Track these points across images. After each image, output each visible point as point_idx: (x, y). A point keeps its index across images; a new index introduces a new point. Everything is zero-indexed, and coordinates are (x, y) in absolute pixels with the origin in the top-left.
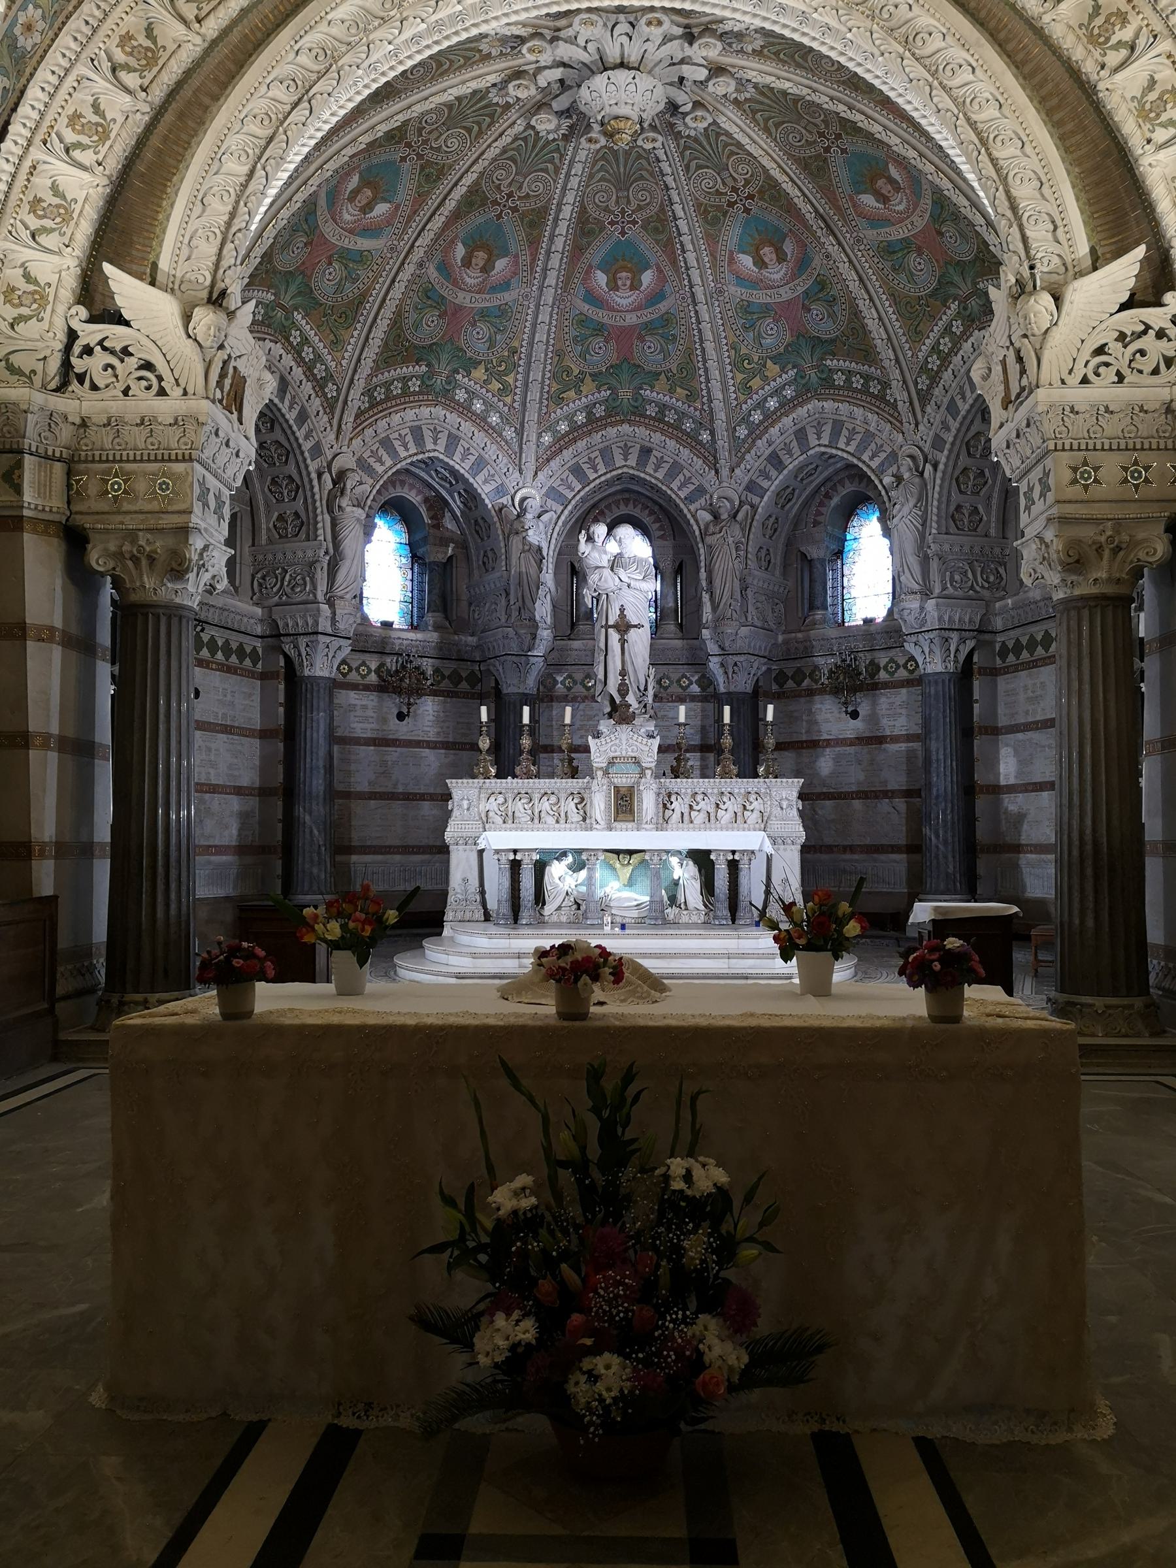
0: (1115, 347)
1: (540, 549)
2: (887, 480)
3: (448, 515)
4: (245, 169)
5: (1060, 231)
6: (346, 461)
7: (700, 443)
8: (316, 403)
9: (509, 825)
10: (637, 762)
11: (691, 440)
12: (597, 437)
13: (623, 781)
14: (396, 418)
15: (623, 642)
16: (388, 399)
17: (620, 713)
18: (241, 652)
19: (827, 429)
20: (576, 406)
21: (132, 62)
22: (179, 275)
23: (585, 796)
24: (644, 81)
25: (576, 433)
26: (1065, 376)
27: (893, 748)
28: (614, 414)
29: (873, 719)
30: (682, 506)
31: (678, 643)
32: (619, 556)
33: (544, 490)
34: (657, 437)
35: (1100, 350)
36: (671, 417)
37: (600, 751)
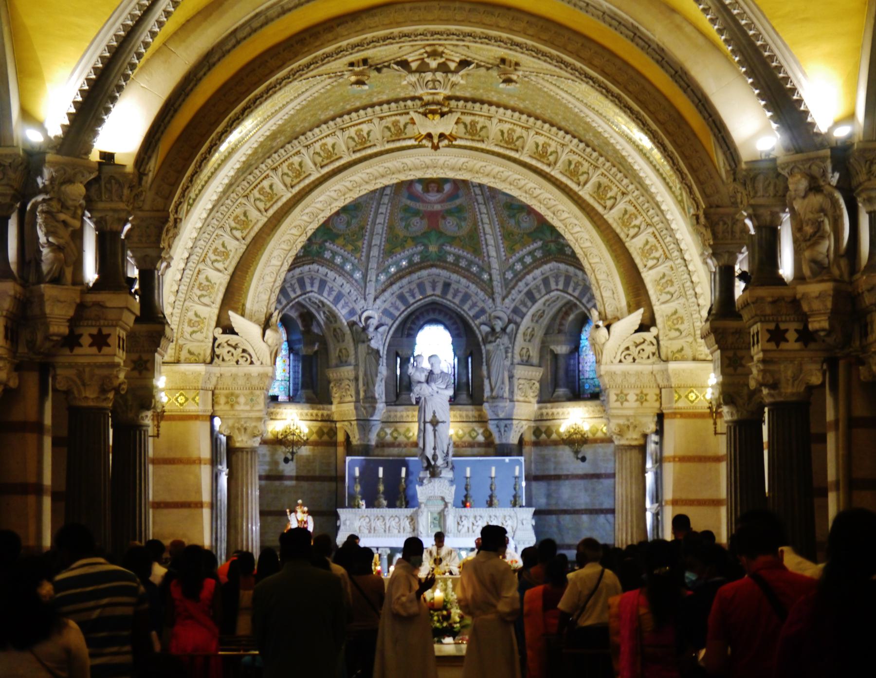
0: (632, 348)
1: (378, 352)
3: (315, 323)
4: (280, 263)
5: (615, 295)
7: (483, 280)
9: (372, 534)
10: (443, 499)
11: (476, 279)
12: (415, 276)
15: (435, 431)
17: (434, 473)
21: (238, 226)
22: (254, 309)
23: (415, 518)
25: (401, 274)
26: (613, 359)
28: (426, 262)
30: (471, 321)
32: (431, 372)
33: (380, 311)
34: (454, 277)
35: (628, 348)
36: (463, 264)
37: (422, 492)
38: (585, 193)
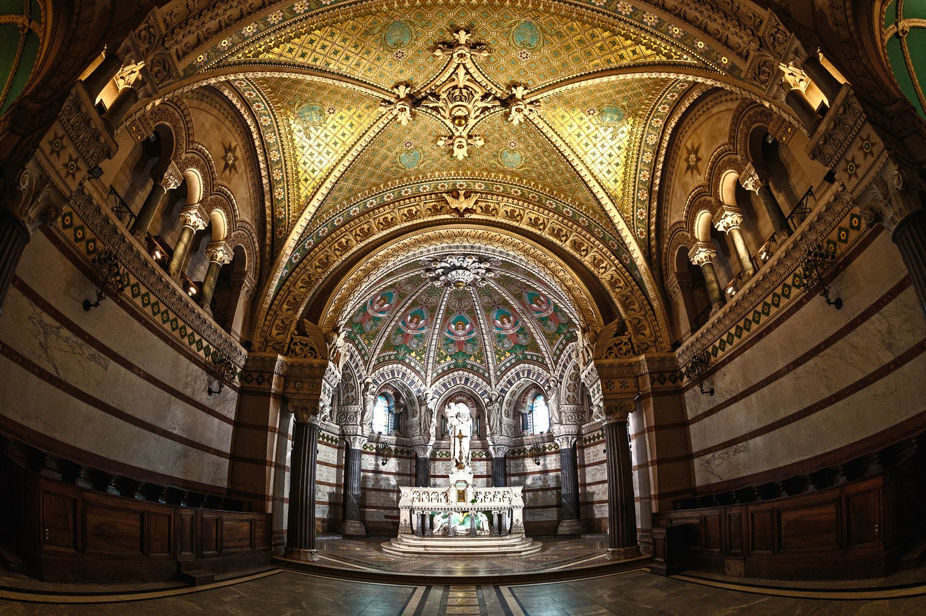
2: (546, 388)
6: (369, 380)
8: (361, 362)
10: (465, 482)
11: (482, 376)
12: (451, 375)
13: (461, 489)
14: (386, 367)
15: (461, 442)
16: (384, 361)
18: (332, 439)
19: (526, 372)
20: (444, 364)
24: (467, 273)
25: (444, 373)
27: (551, 474)
28: (457, 368)
29: (545, 465)
31: (479, 442)
34: (471, 375)
36: (475, 369)
38: (567, 246)
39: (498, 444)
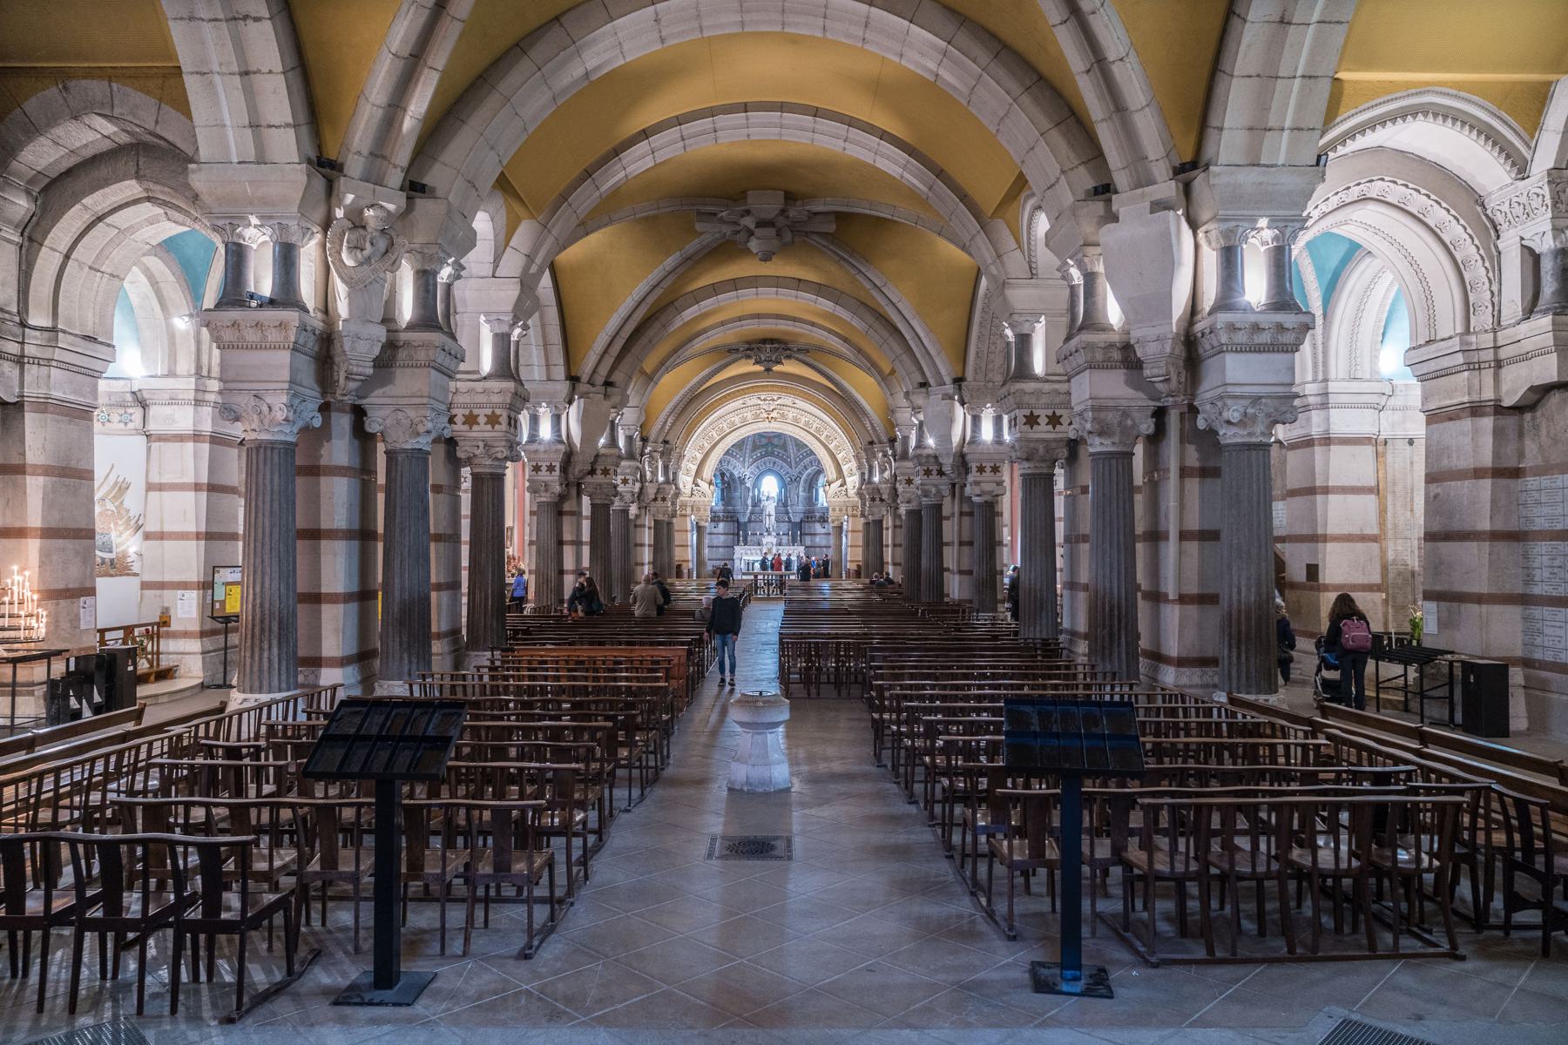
11: (785, 461)
37: (765, 541)
38: (822, 438)
39: (797, 511)
